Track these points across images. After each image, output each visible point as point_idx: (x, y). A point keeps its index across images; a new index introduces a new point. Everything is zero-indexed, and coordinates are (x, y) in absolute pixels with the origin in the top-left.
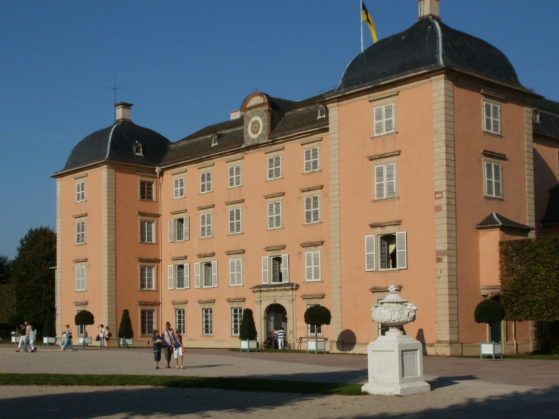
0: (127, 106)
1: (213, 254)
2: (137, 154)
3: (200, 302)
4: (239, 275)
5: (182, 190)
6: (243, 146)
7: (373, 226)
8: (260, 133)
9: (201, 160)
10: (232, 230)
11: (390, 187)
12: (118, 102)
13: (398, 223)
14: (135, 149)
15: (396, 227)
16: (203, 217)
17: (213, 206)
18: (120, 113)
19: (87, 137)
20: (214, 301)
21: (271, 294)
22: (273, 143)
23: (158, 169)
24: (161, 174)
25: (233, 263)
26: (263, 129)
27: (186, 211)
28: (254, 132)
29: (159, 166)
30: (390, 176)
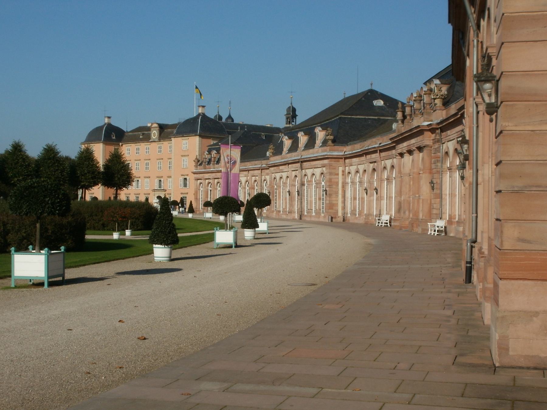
0: (109, 118)
1: (140, 177)
2: (113, 138)
3: (135, 194)
4: (148, 185)
5: (129, 152)
6: (150, 141)
7: (182, 175)
8: (156, 137)
9: (136, 143)
10: (146, 169)
11: (186, 165)
12: (106, 116)
13: (188, 175)
14: (112, 136)
15: (187, 176)
16: (137, 163)
17: (140, 160)
18: (106, 120)
19: (94, 129)
20: (140, 194)
21: (158, 192)
22: (160, 141)
23: (120, 144)
24: (122, 145)
25: (146, 181)
26: (157, 136)
27: (130, 160)
28: (154, 136)
29: (121, 143)
30: (186, 162)
